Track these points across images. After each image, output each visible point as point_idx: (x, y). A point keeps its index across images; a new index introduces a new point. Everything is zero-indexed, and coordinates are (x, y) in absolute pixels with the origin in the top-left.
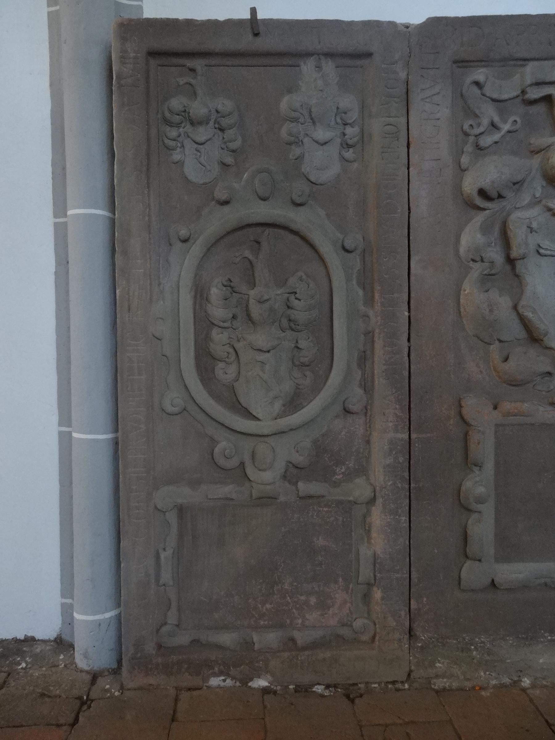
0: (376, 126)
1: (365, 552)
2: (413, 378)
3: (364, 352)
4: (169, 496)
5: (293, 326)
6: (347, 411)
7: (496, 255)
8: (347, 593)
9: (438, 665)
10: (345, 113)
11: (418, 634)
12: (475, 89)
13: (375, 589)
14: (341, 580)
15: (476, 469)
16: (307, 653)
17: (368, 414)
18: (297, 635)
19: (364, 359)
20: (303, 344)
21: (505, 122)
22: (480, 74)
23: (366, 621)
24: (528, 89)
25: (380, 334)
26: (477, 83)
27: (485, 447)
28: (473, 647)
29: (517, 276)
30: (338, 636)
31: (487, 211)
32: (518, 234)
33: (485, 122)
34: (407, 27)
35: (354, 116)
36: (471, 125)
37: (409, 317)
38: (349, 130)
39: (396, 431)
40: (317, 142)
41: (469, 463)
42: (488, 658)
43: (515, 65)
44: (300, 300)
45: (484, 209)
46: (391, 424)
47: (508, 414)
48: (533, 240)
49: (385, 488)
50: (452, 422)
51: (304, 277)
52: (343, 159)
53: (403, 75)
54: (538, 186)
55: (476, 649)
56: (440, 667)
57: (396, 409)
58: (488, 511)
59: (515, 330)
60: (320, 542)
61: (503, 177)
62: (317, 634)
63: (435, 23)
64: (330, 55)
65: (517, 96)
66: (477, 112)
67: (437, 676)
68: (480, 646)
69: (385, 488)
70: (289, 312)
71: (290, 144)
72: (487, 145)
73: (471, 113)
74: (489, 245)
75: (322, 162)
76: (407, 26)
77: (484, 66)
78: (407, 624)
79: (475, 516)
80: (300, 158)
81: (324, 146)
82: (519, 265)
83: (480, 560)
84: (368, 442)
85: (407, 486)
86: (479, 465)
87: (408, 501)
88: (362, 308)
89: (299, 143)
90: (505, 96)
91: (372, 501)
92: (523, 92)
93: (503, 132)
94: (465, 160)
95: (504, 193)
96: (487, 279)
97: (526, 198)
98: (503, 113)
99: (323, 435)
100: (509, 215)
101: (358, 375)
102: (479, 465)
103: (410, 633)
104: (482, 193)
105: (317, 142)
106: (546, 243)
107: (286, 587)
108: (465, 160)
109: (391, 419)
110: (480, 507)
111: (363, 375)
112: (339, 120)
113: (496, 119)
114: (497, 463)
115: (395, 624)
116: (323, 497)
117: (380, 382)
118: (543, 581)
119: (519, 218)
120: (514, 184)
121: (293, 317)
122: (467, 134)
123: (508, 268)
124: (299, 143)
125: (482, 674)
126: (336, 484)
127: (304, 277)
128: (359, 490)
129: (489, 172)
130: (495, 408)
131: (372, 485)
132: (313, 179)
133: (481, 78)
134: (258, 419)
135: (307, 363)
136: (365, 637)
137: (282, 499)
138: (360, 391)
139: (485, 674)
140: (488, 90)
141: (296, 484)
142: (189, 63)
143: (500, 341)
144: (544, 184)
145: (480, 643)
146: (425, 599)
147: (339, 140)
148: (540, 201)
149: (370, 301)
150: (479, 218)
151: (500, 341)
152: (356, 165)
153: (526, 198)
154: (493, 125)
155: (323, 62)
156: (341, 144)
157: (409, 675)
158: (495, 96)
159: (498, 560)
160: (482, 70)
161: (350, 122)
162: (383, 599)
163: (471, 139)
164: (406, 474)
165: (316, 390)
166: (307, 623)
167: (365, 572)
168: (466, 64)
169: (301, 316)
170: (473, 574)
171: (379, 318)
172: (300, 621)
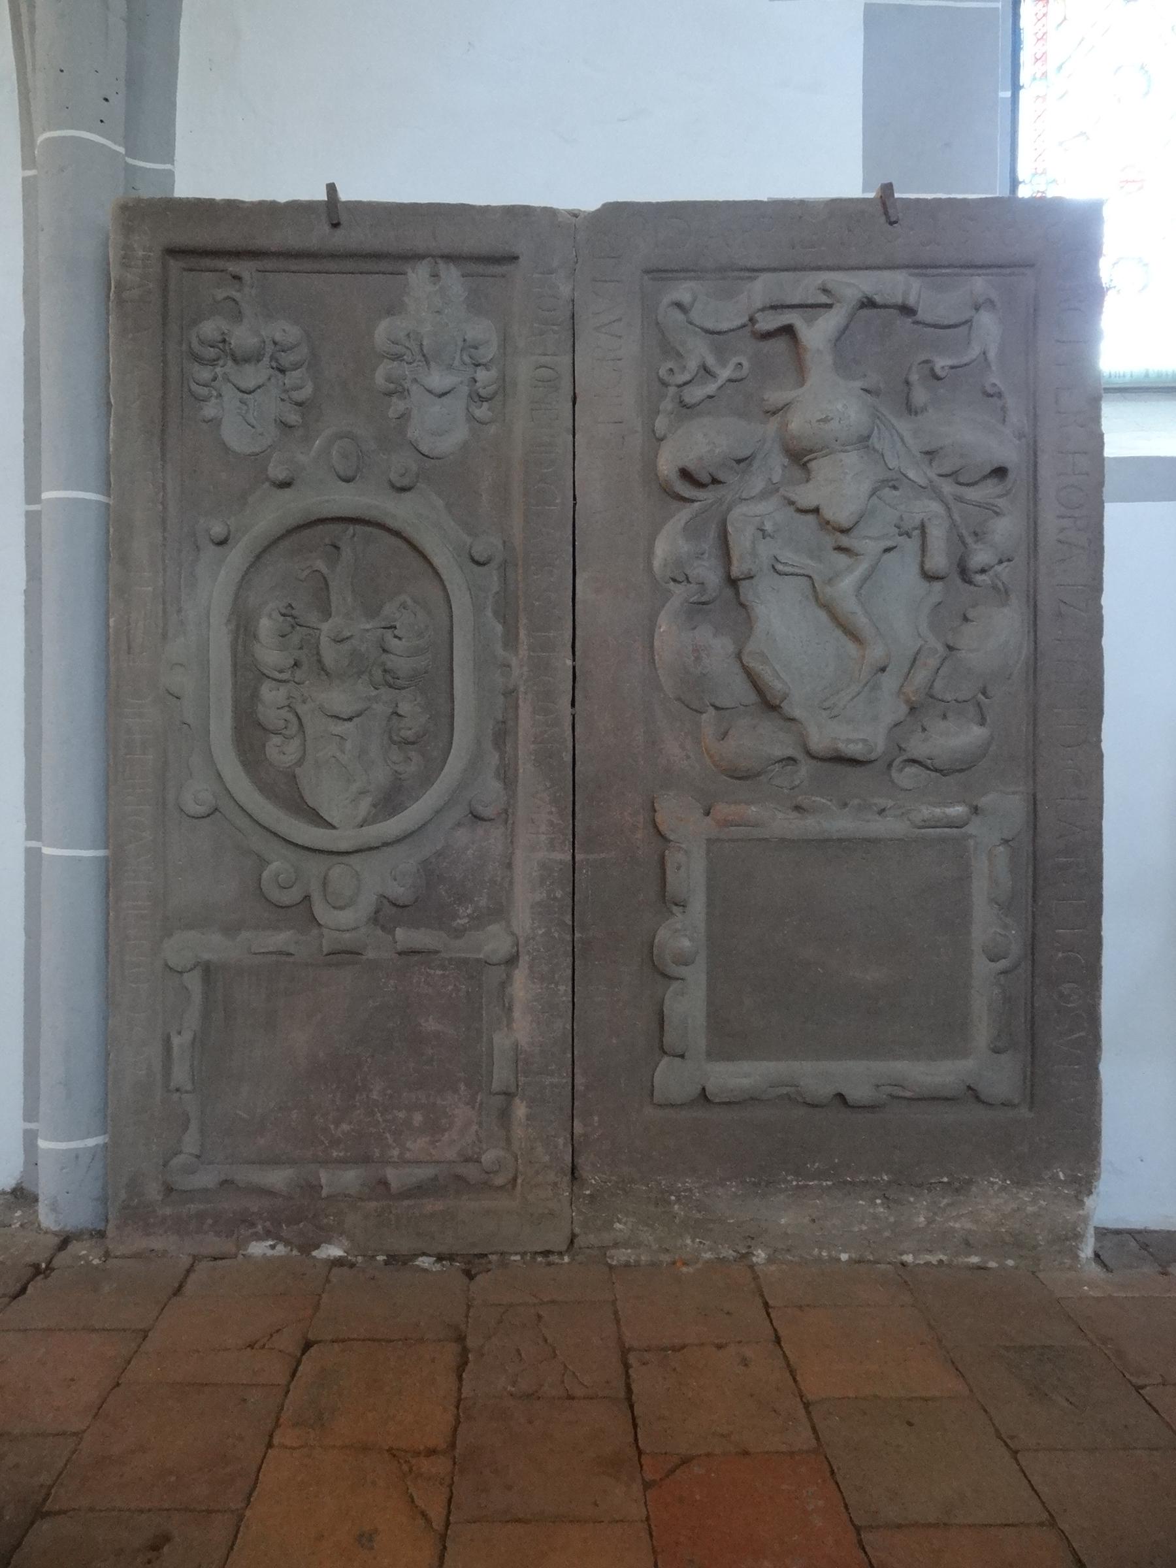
0: (523, 370)
1: (501, 1041)
2: (578, 764)
3: (504, 722)
4: (186, 947)
5: (391, 680)
6: (477, 817)
7: (709, 572)
8: (473, 1108)
9: (618, 1226)
10: (476, 348)
11: (585, 1175)
12: (679, 316)
13: (517, 1101)
14: (462, 1087)
15: (675, 909)
16: (406, 1203)
17: (510, 822)
18: (391, 1174)
19: (503, 735)
20: (405, 708)
21: (723, 363)
22: (683, 291)
23: (502, 1153)
24: (759, 316)
25: (526, 693)
26: (679, 305)
27: (690, 873)
28: (673, 1198)
29: (742, 605)
30: (458, 1178)
31: (696, 504)
32: (742, 540)
33: (693, 365)
34: (576, 216)
35: (489, 352)
36: (671, 370)
37: (574, 667)
38: (482, 375)
39: (552, 846)
40: (430, 392)
41: (668, 902)
42: (698, 1216)
43: (742, 279)
44: (400, 639)
45: (693, 501)
46: (543, 837)
47: (726, 823)
48: (766, 550)
49: (533, 939)
50: (639, 836)
51: (409, 602)
52: (471, 418)
53: (565, 290)
54: (777, 464)
55: (678, 1199)
56: (621, 1231)
57: (551, 813)
58: (696, 977)
59: (738, 691)
60: (431, 1025)
61: (717, 451)
62: (423, 1173)
63: (616, 213)
64: (449, 258)
65: (744, 326)
66: (681, 350)
67: (616, 1245)
68: (685, 1197)
69: (533, 939)
70: (384, 656)
71: (390, 394)
72: (693, 401)
73: (669, 350)
74: (700, 556)
75: (439, 423)
76: (575, 214)
77: (694, 278)
78: (568, 1158)
79: (675, 985)
80: (404, 417)
81: (444, 399)
82: (744, 586)
83: (682, 1056)
84: (509, 866)
85: (569, 938)
86: (682, 905)
87: (569, 960)
88: (500, 651)
89: (403, 393)
90: (724, 326)
91: (512, 961)
92: (752, 320)
93: (720, 382)
94: (661, 424)
95: (721, 477)
96: (697, 609)
97: (758, 484)
98: (721, 354)
99: (439, 854)
100: (729, 510)
101: (494, 759)
102: (682, 905)
103: (573, 1173)
104: (685, 474)
105: (430, 392)
106: (787, 555)
107: (375, 1096)
108: (661, 424)
109: (543, 828)
110: (682, 971)
111: (502, 758)
112: (467, 359)
113: (711, 361)
114: (710, 904)
115: (547, 1158)
116: (437, 952)
117: (526, 769)
118: (785, 1090)
119: (745, 515)
120: (739, 461)
121: (389, 665)
122: (665, 384)
123: (728, 592)
124: (403, 393)
125: (689, 1241)
126: (459, 933)
127: (409, 602)
128: (493, 942)
129: (697, 443)
130: (707, 814)
131: (513, 934)
132: (425, 450)
133: (686, 298)
134: (334, 827)
135: (412, 739)
136: (499, 1181)
137: (370, 954)
138: (496, 785)
139: (693, 1241)
140: (695, 315)
141: (391, 932)
142: (233, 267)
143: (717, 708)
144: (786, 461)
145: (685, 1191)
146: (596, 1118)
147: (465, 389)
148: (777, 490)
149: (511, 641)
150: (685, 513)
151: (717, 708)
152: (493, 429)
153: (758, 484)
154: (706, 371)
155: (442, 265)
156: (470, 396)
157: (572, 1242)
158: (710, 325)
159: (710, 1055)
160: (692, 284)
161: (484, 361)
162: (528, 1117)
163: (672, 390)
164: (568, 919)
165: (427, 779)
166: (408, 1155)
167: (501, 1076)
168: (664, 275)
169: (402, 664)
170: (673, 1080)
171: (525, 669)
172: (396, 1152)
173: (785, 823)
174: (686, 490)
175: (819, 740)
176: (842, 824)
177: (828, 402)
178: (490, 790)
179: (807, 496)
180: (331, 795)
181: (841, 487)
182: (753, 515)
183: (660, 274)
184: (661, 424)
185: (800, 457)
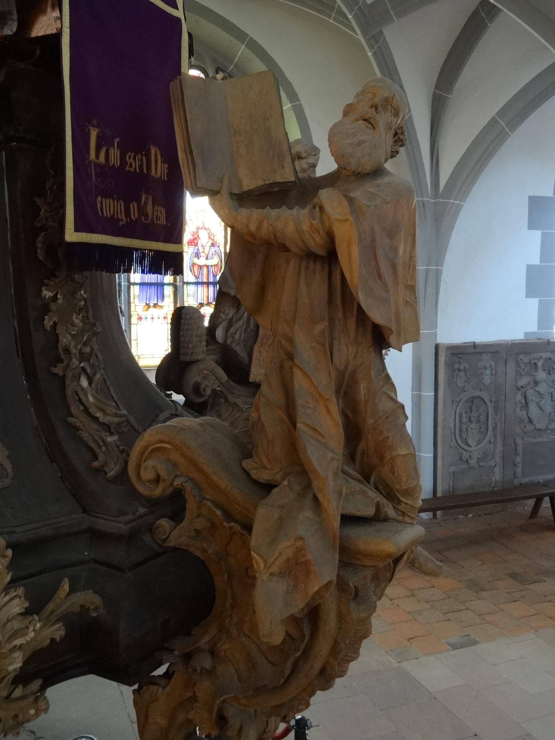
4: (453, 469)
7: (524, 402)
27: (520, 449)
41: (516, 454)
54: (532, 384)
58: (520, 465)
59: (527, 420)
86: (519, 455)
97: (530, 387)
104: (522, 387)
117: (498, 436)
129: (523, 381)
142: (459, 356)
153: (530, 387)
173: (533, 440)
174: (521, 389)
175: (537, 428)
176: (540, 440)
177: (541, 375)
178: (493, 438)
179: (537, 389)
180: (470, 441)
181: (542, 388)
182: (530, 392)
183: (517, 354)
184: (518, 378)
185: (536, 383)
